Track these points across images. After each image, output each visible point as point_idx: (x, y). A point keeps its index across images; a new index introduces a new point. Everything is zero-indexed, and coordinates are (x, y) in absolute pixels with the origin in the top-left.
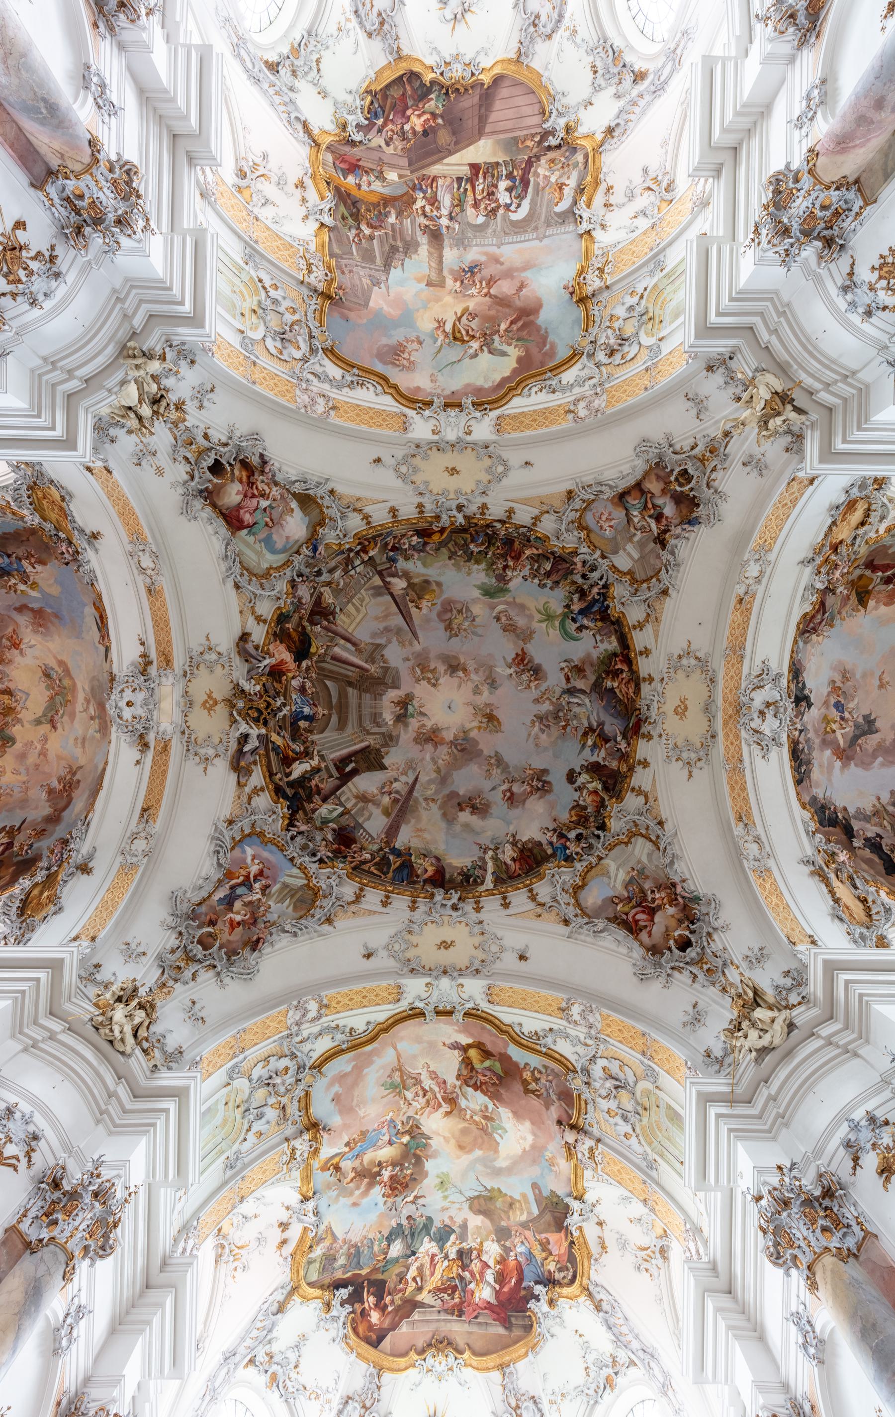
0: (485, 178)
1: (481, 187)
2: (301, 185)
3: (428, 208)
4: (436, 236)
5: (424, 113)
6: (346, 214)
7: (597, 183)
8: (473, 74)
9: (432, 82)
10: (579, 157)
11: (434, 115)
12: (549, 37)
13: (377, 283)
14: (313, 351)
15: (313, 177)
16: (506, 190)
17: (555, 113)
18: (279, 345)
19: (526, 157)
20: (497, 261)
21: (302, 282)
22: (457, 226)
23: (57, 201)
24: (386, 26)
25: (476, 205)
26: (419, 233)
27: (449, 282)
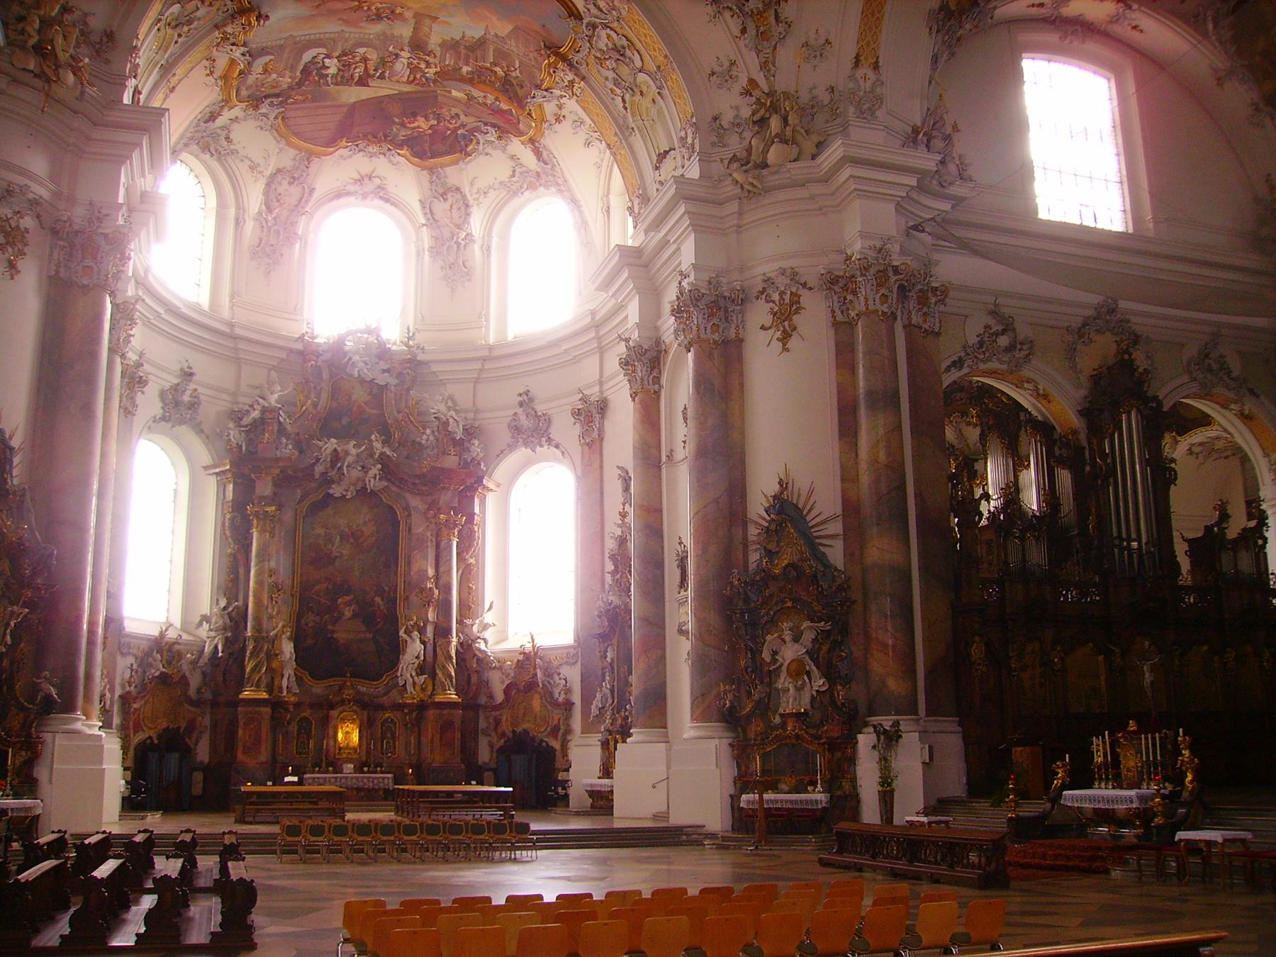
0: (352, 76)
1: (358, 70)
2: (558, 120)
3: (423, 66)
4: (418, 46)
5: (414, 128)
6: (518, 89)
7: (225, 78)
8: (357, 145)
9: (401, 146)
10: (244, 93)
11: (403, 125)
12: (279, 171)
13: (496, 35)
14: (593, 26)
15: (543, 120)
16: (328, 68)
17: (272, 116)
18: (628, 53)
19: (304, 88)
20: (346, 22)
21: (583, 79)
22: (391, 49)
23: (733, 326)
24: (441, 191)
25: (365, 60)
26: (438, 54)
27: (409, 14)
